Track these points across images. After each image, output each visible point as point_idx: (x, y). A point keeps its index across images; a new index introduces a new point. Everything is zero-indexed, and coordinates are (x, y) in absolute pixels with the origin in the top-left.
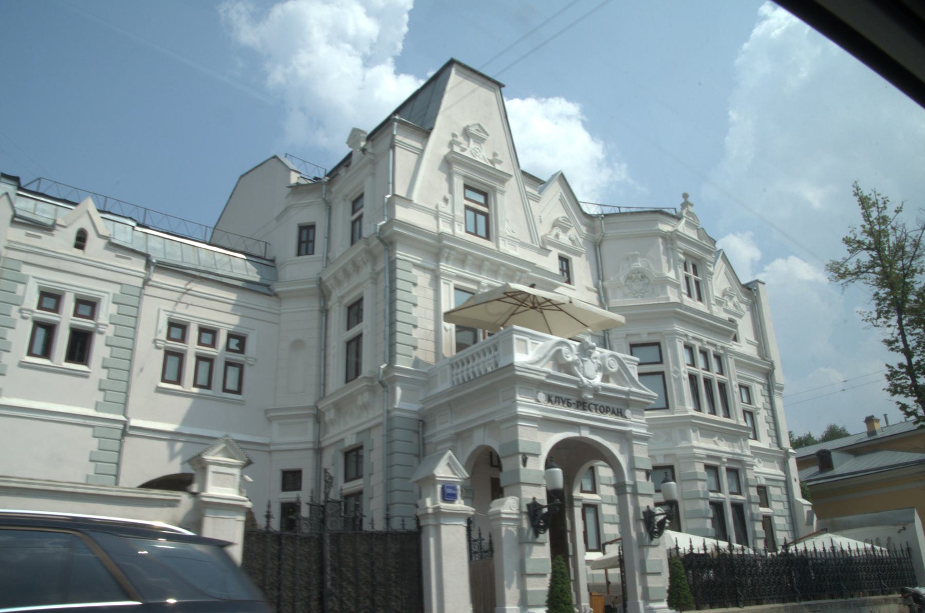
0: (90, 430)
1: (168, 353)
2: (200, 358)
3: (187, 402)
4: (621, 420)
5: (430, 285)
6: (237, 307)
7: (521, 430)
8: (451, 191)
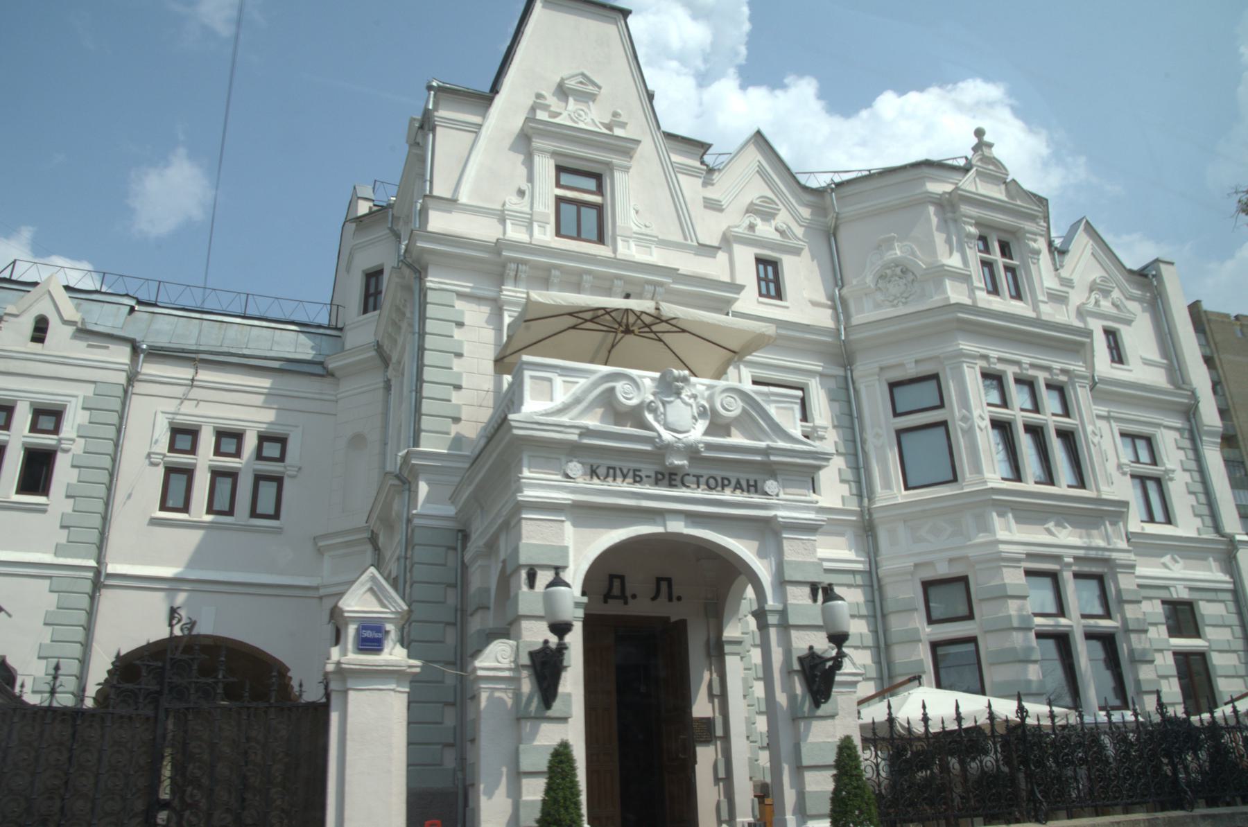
0: (47, 582)
1: (170, 470)
2: (216, 474)
3: (196, 536)
4: (757, 499)
5: (488, 322)
6: (271, 396)
7: (526, 528)
8: (530, 179)
